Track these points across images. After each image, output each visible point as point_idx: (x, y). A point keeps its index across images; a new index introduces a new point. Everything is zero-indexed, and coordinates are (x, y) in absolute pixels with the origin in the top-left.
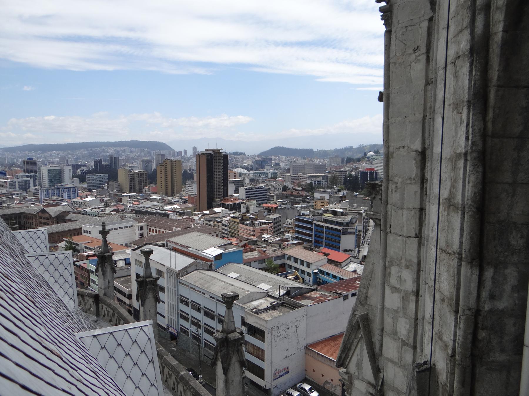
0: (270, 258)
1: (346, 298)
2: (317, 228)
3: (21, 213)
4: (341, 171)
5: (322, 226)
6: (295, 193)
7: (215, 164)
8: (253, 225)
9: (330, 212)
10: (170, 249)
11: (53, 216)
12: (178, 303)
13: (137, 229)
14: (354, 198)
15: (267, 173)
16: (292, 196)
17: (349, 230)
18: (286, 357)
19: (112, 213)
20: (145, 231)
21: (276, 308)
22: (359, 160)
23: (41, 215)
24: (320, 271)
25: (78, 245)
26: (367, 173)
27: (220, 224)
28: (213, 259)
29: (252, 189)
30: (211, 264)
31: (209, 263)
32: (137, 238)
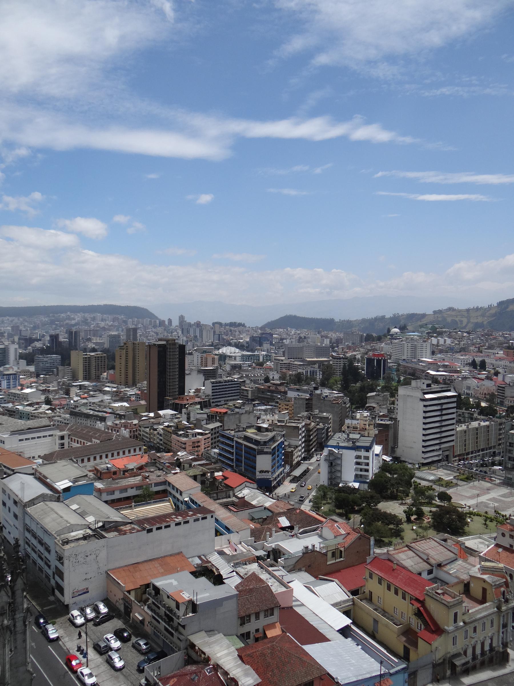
0: (149, 484)
1: (150, 531)
2: (238, 445)
4: (340, 359)
5: (241, 444)
7: (168, 357)
8: (187, 436)
9: (255, 427)
10: (35, 478)
12: (24, 531)
13: (57, 438)
14: (322, 401)
15: (258, 356)
17: (265, 450)
18: (86, 579)
19: (47, 412)
20: (66, 441)
21: (87, 538)
22: (379, 339)
26: (374, 359)
27: (156, 432)
28: (62, 492)
29: (220, 382)
30: (60, 496)
31: (57, 495)
32: (57, 448)
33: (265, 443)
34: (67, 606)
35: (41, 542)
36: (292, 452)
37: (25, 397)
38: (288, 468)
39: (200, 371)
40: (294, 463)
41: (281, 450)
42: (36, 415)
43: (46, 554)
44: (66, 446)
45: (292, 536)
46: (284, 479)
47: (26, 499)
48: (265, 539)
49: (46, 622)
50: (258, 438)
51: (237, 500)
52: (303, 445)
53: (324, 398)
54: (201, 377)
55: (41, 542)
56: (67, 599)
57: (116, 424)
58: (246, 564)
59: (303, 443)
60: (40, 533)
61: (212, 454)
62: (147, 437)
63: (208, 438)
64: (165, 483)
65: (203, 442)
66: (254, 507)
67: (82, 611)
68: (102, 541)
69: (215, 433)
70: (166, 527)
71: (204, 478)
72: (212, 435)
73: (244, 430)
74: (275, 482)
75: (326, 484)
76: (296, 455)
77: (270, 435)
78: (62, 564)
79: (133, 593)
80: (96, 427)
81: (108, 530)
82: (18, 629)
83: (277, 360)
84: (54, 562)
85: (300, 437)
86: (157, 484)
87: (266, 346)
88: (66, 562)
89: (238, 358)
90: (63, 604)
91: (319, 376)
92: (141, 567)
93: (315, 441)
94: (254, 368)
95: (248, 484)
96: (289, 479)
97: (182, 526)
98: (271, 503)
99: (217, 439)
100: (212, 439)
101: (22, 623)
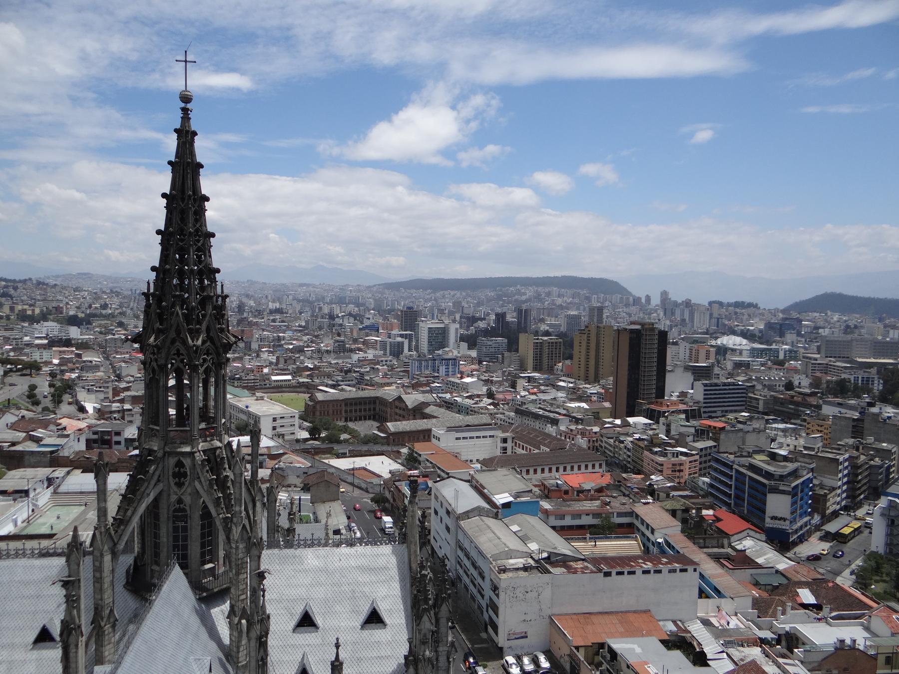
1: (607, 574)
2: (739, 476)
3: (377, 398)
6: (798, 399)
8: (664, 455)
9: (766, 453)
10: (471, 486)
11: (410, 407)
13: (499, 440)
15: (777, 351)
16: (792, 403)
17: (781, 488)
20: (509, 445)
23: (397, 403)
24: (667, 542)
25: (420, 455)
27: (622, 445)
29: (716, 385)
32: (498, 452)
33: (782, 478)
34: (501, 649)
35: (474, 565)
36: (826, 495)
37: (465, 387)
38: (817, 519)
39: (687, 368)
40: (828, 512)
41: (806, 490)
42: (476, 409)
43: (479, 580)
44: (509, 452)
45: (819, 619)
46: (809, 533)
47: (460, 510)
48: (774, 615)
49: (476, 663)
50: (771, 469)
51: (734, 553)
52: (845, 487)
53: (885, 420)
54: (689, 377)
55: (474, 565)
56: (502, 640)
57: (571, 430)
58: (743, 646)
59: (844, 484)
60: (473, 553)
61: (700, 484)
62: (610, 451)
63: (695, 461)
64: (631, 514)
65: (687, 466)
66: (759, 566)
67: (519, 658)
68: (546, 577)
69: (706, 455)
70: (630, 573)
71: (686, 515)
72: (701, 457)
73: (750, 455)
74: (795, 537)
75: (881, 550)
76: (832, 501)
77: (791, 466)
78: (498, 596)
79: (582, 650)
80: (546, 431)
81: (554, 564)
82: (440, 665)
83: (807, 358)
84: (488, 593)
85: (840, 475)
86: (620, 515)
87: (790, 337)
88: (502, 595)
89: (744, 353)
90: (497, 645)
91: (878, 386)
92: (594, 619)
93: (865, 484)
94: (770, 368)
95: (752, 533)
96: (818, 534)
97: (652, 576)
98: (786, 566)
99: (708, 464)
100: (701, 463)
101: (445, 658)
